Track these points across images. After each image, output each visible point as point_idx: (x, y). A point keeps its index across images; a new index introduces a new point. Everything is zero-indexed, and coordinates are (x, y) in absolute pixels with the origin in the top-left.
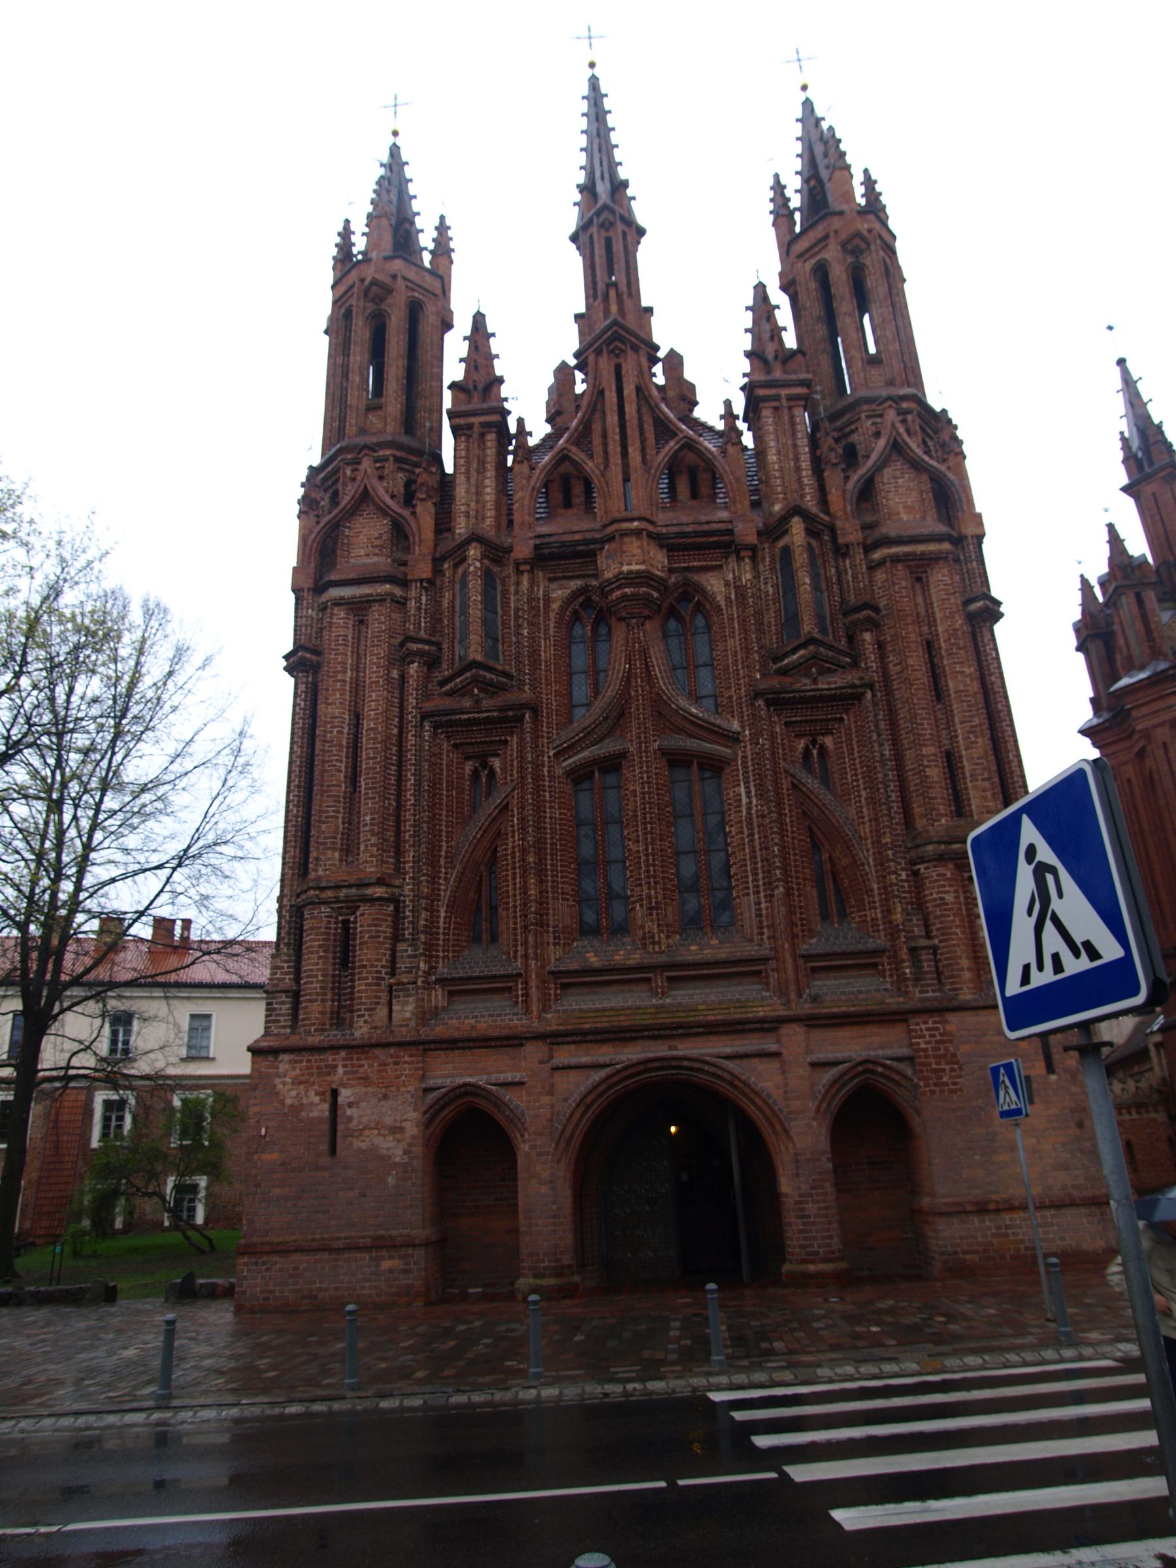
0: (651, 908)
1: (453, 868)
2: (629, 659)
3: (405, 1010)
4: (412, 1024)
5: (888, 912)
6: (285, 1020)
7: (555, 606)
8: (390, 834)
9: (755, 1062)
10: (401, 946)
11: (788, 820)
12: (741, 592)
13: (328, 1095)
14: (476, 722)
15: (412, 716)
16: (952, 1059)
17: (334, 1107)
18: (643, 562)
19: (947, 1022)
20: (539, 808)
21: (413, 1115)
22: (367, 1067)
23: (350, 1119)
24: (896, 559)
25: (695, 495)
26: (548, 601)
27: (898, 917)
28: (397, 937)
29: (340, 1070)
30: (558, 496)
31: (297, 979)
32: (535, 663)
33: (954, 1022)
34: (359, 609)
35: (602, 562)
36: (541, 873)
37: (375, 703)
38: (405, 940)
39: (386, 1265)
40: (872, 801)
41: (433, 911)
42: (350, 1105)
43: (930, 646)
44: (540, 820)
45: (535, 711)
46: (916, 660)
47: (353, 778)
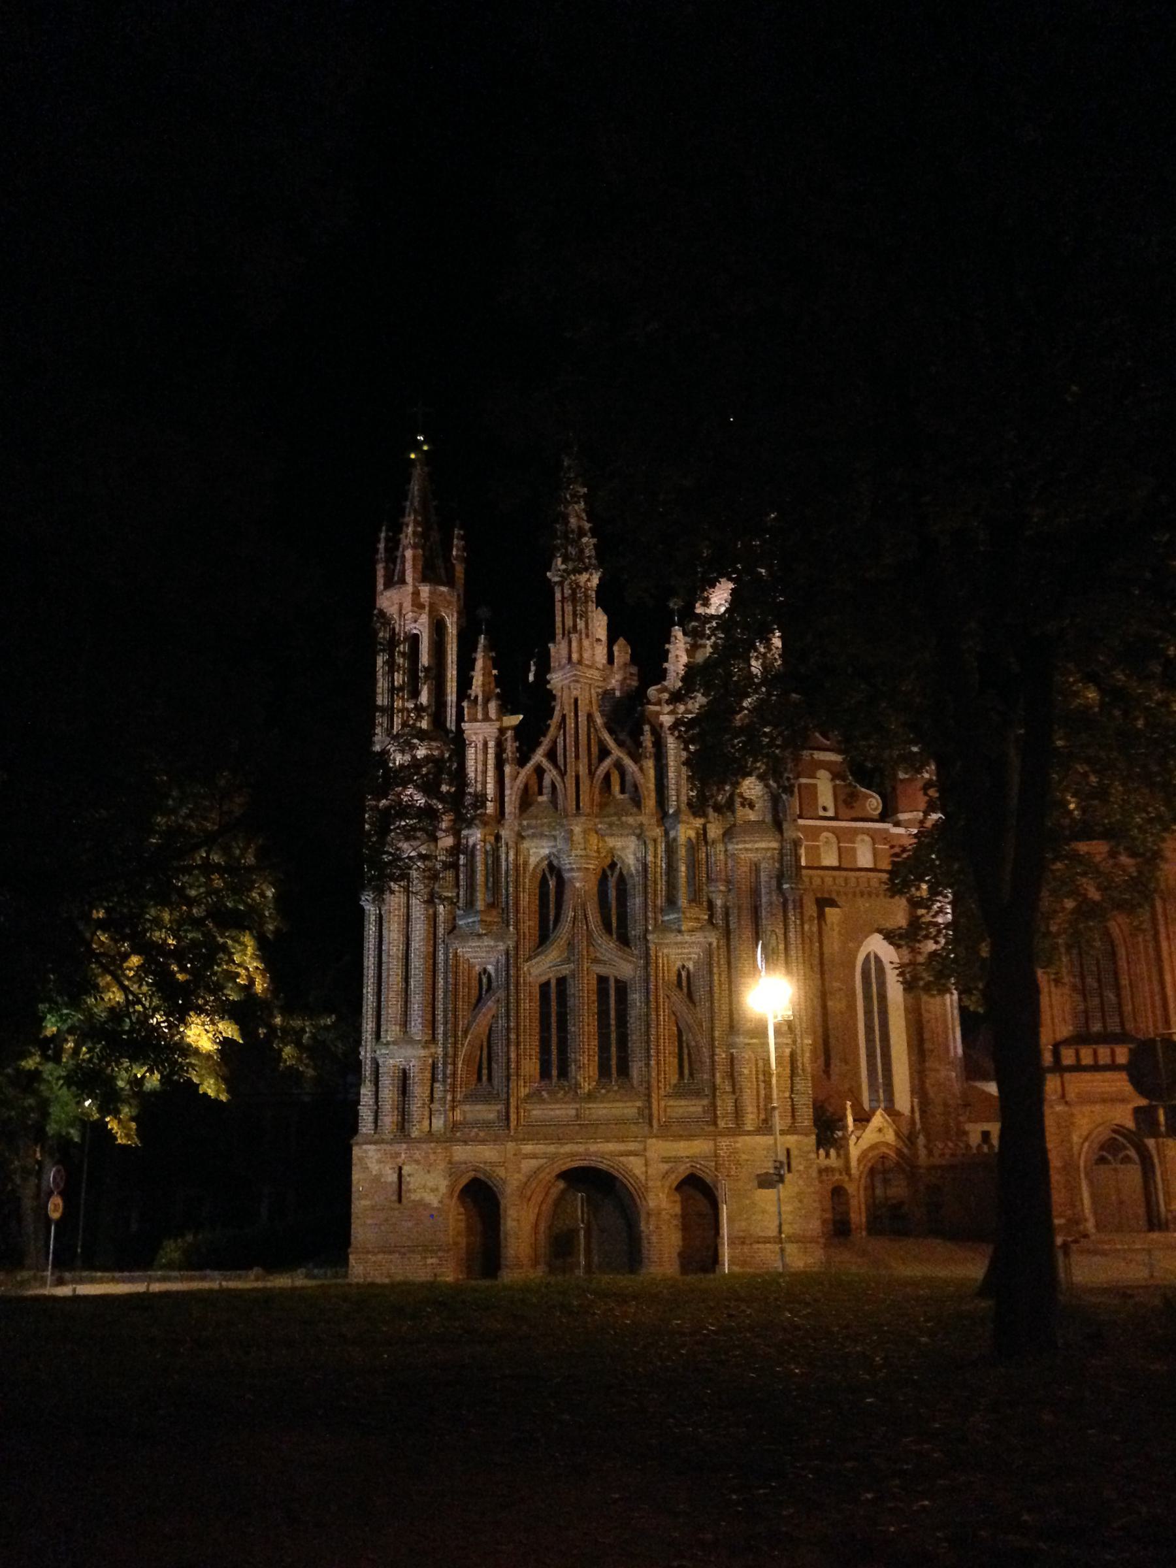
0: (580, 1067)
1: (466, 1037)
2: (574, 910)
3: (438, 1123)
4: (443, 1130)
5: (714, 1076)
9: (631, 1158)
10: (437, 1085)
11: (662, 1018)
13: (397, 1170)
16: (738, 1163)
17: (400, 1176)
18: (585, 849)
19: (737, 1142)
20: (518, 1001)
23: (408, 1183)
25: (623, 791)
26: (526, 863)
27: (718, 1080)
28: (434, 1079)
29: (403, 1155)
31: (377, 1102)
33: (743, 1142)
36: (518, 1044)
38: (438, 1081)
39: (429, 1261)
41: (454, 1064)
42: (409, 1175)
44: (517, 1012)
47: (406, 979)
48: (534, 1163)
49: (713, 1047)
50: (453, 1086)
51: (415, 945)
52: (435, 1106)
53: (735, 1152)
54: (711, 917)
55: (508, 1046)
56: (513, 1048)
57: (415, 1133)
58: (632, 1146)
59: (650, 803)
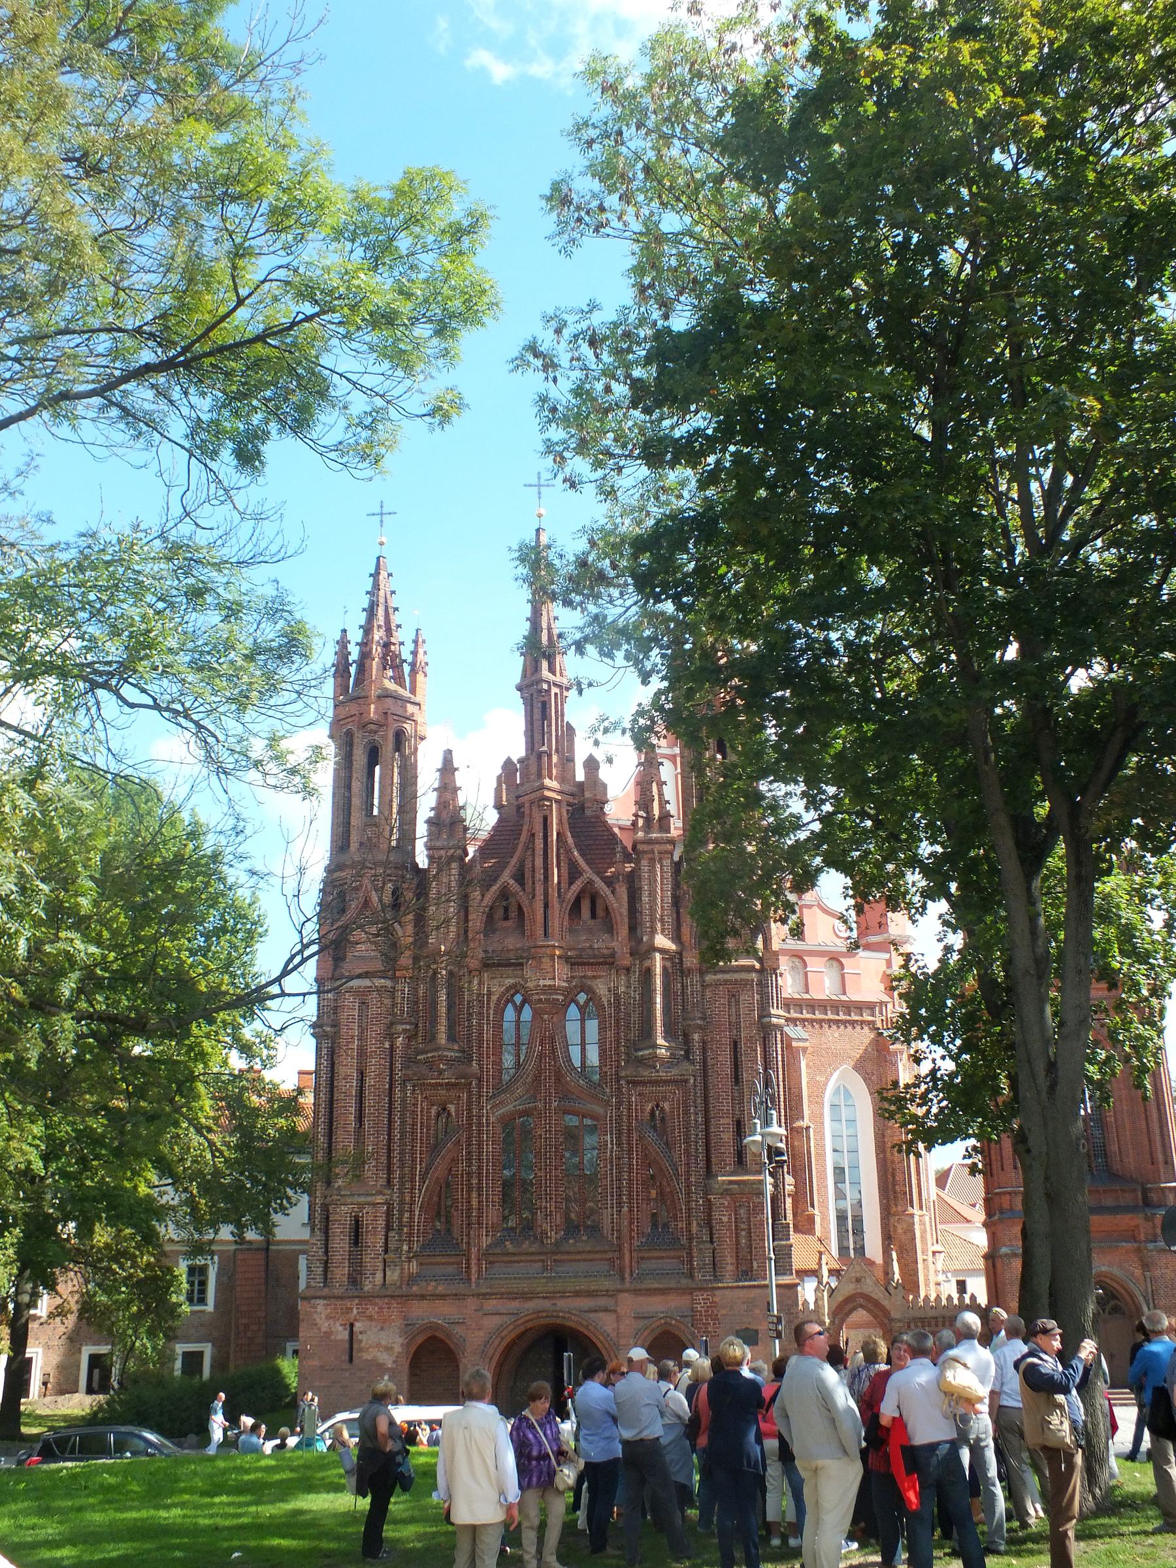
2: (541, 1044)
3: (393, 1275)
5: (689, 1224)
6: (320, 1279)
7: (494, 998)
8: (384, 1159)
9: (601, 1315)
10: (391, 1234)
12: (617, 997)
14: (441, 1085)
15: (399, 1075)
16: (715, 1318)
20: (480, 1145)
21: (400, 1340)
22: (372, 1310)
24: (717, 984)
25: (594, 915)
26: (489, 994)
28: (388, 1228)
30: (500, 913)
32: (480, 1041)
34: (362, 994)
35: (528, 972)
36: (480, 1189)
37: (375, 1066)
40: (687, 1151)
41: (411, 1211)
43: (735, 1044)
44: (480, 1153)
45: (480, 1080)
46: (724, 1058)
48: (496, 1321)
49: (688, 1193)
50: (410, 1234)
51: (369, 1081)
52: (391, 1255)
53: (714, 1305)
54: (687, 1052)
55: (469, 1191)
56: (474, 1195)
57: (368, 1287)
58: (603, 1302)
59: (623, 931)
